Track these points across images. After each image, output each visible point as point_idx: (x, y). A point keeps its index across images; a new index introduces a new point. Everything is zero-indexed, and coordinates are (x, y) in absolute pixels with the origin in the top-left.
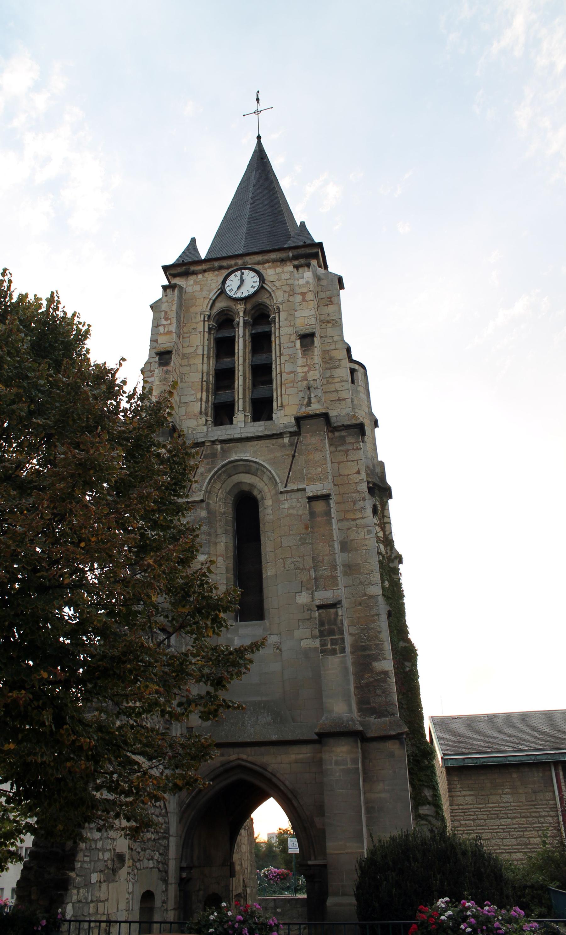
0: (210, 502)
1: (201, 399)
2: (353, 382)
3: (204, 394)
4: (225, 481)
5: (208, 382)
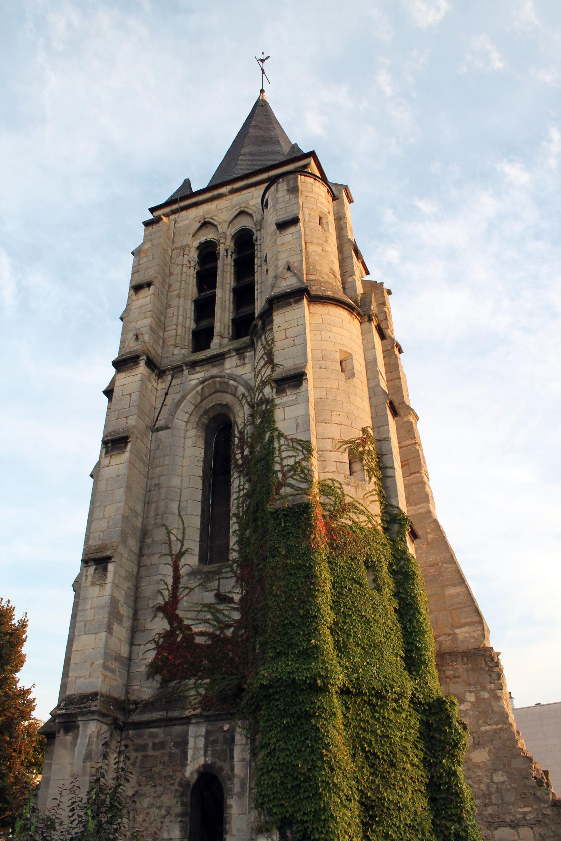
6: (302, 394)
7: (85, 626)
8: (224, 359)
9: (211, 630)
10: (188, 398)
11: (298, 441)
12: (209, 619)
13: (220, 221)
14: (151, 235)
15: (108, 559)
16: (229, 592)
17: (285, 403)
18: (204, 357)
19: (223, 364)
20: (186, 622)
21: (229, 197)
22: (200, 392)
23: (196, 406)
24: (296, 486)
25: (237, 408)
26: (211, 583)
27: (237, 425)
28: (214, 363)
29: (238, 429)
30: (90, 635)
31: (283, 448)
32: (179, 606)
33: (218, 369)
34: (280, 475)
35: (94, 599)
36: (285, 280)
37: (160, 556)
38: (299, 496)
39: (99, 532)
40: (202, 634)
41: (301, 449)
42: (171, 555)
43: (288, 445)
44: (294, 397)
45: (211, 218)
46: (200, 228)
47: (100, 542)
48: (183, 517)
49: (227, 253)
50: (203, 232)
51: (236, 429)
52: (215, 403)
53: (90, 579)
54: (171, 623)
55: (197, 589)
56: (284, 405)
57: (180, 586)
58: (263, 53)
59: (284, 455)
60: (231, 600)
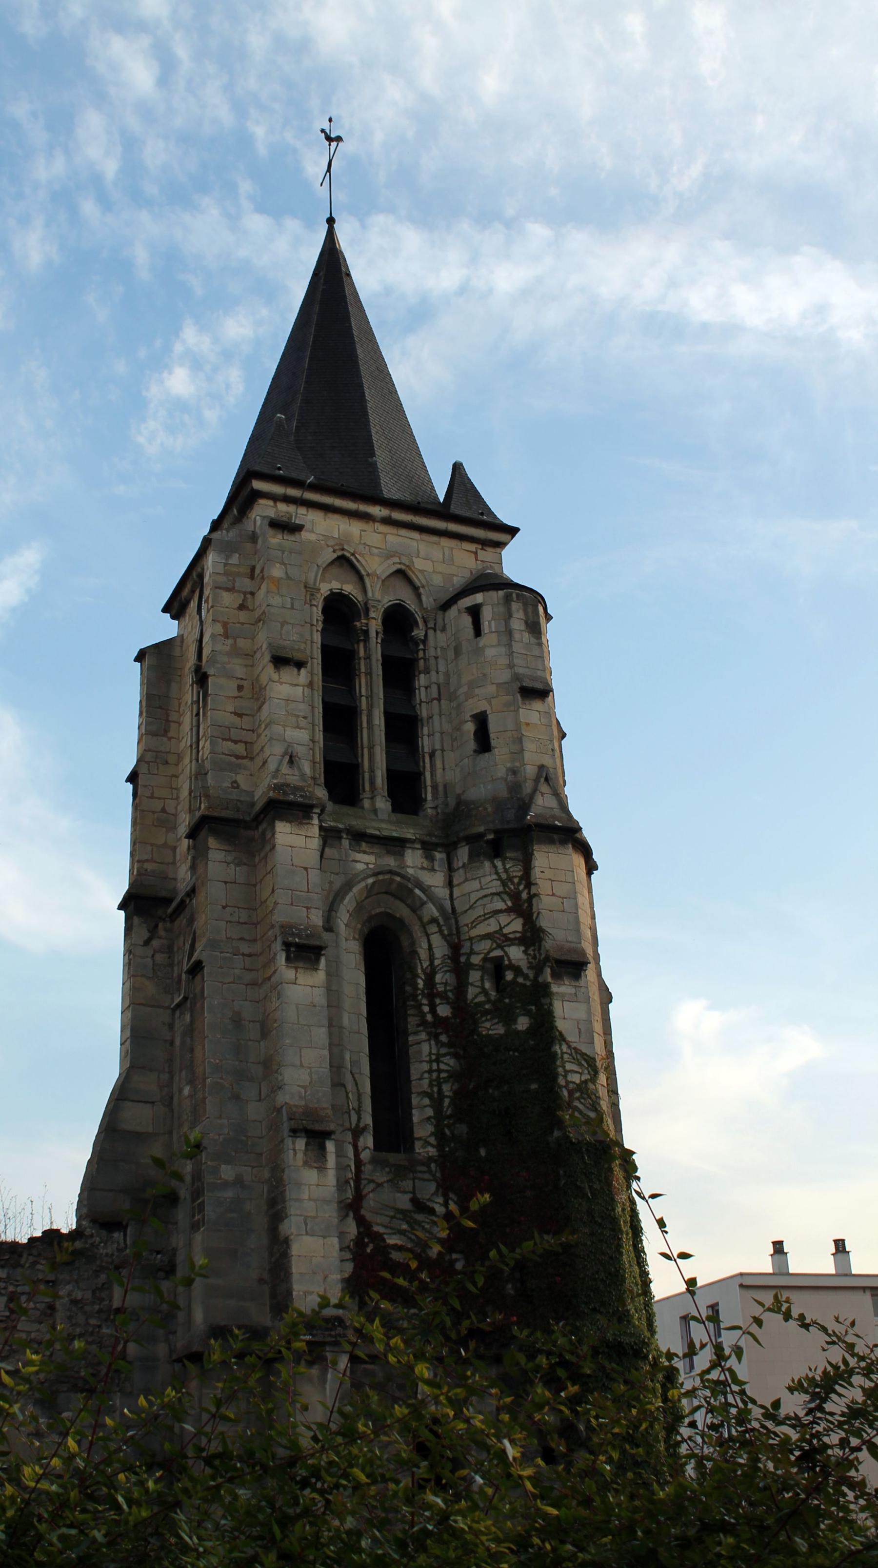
2: (478, 632)
6: (583, 990)
7: (306, 1224)
9: (409, 1246)
10: (355, 889)
11: (583, 1055)
12: (405, 1231)
13: (370, 572)
14: (283, 552)
15: (327, 1135)
16: (429, 1200)
18: (377, 833)
19: (402, 855)
20: (376, 1228)
21: (377, 525)
22: (369, 887)
23: (358, 904)
24: (585, 1112)
25: (417, 932)
26: (404, 1182)
27: (420, 961)
30: (315, 1238)
31: (566, 1056)
32: (365, 1204)
33: (395, 860)
34: (565, 1093)
35: (312, 1187)
36: (542, 796)
37: (343, 1131)
39: (299, 1086)
40: (399, 1248)
41: (586, 1066)
42: (350, 1129)
43: (571, 1055)
44: (573, 991)
45: (353, 554)
46: (332, 563)
47: (303, 1103)
48: (356, 1076)
49: (377, 639)
50: (335, 570)
51: (419, 964)
52: (382, 910)
53: (300, 1156)
54: (358, 1226)
55: (385, 1185)
56: (563, 998)
57: (363, 1177)
59: (568, 1066)
60: (432, 1211)
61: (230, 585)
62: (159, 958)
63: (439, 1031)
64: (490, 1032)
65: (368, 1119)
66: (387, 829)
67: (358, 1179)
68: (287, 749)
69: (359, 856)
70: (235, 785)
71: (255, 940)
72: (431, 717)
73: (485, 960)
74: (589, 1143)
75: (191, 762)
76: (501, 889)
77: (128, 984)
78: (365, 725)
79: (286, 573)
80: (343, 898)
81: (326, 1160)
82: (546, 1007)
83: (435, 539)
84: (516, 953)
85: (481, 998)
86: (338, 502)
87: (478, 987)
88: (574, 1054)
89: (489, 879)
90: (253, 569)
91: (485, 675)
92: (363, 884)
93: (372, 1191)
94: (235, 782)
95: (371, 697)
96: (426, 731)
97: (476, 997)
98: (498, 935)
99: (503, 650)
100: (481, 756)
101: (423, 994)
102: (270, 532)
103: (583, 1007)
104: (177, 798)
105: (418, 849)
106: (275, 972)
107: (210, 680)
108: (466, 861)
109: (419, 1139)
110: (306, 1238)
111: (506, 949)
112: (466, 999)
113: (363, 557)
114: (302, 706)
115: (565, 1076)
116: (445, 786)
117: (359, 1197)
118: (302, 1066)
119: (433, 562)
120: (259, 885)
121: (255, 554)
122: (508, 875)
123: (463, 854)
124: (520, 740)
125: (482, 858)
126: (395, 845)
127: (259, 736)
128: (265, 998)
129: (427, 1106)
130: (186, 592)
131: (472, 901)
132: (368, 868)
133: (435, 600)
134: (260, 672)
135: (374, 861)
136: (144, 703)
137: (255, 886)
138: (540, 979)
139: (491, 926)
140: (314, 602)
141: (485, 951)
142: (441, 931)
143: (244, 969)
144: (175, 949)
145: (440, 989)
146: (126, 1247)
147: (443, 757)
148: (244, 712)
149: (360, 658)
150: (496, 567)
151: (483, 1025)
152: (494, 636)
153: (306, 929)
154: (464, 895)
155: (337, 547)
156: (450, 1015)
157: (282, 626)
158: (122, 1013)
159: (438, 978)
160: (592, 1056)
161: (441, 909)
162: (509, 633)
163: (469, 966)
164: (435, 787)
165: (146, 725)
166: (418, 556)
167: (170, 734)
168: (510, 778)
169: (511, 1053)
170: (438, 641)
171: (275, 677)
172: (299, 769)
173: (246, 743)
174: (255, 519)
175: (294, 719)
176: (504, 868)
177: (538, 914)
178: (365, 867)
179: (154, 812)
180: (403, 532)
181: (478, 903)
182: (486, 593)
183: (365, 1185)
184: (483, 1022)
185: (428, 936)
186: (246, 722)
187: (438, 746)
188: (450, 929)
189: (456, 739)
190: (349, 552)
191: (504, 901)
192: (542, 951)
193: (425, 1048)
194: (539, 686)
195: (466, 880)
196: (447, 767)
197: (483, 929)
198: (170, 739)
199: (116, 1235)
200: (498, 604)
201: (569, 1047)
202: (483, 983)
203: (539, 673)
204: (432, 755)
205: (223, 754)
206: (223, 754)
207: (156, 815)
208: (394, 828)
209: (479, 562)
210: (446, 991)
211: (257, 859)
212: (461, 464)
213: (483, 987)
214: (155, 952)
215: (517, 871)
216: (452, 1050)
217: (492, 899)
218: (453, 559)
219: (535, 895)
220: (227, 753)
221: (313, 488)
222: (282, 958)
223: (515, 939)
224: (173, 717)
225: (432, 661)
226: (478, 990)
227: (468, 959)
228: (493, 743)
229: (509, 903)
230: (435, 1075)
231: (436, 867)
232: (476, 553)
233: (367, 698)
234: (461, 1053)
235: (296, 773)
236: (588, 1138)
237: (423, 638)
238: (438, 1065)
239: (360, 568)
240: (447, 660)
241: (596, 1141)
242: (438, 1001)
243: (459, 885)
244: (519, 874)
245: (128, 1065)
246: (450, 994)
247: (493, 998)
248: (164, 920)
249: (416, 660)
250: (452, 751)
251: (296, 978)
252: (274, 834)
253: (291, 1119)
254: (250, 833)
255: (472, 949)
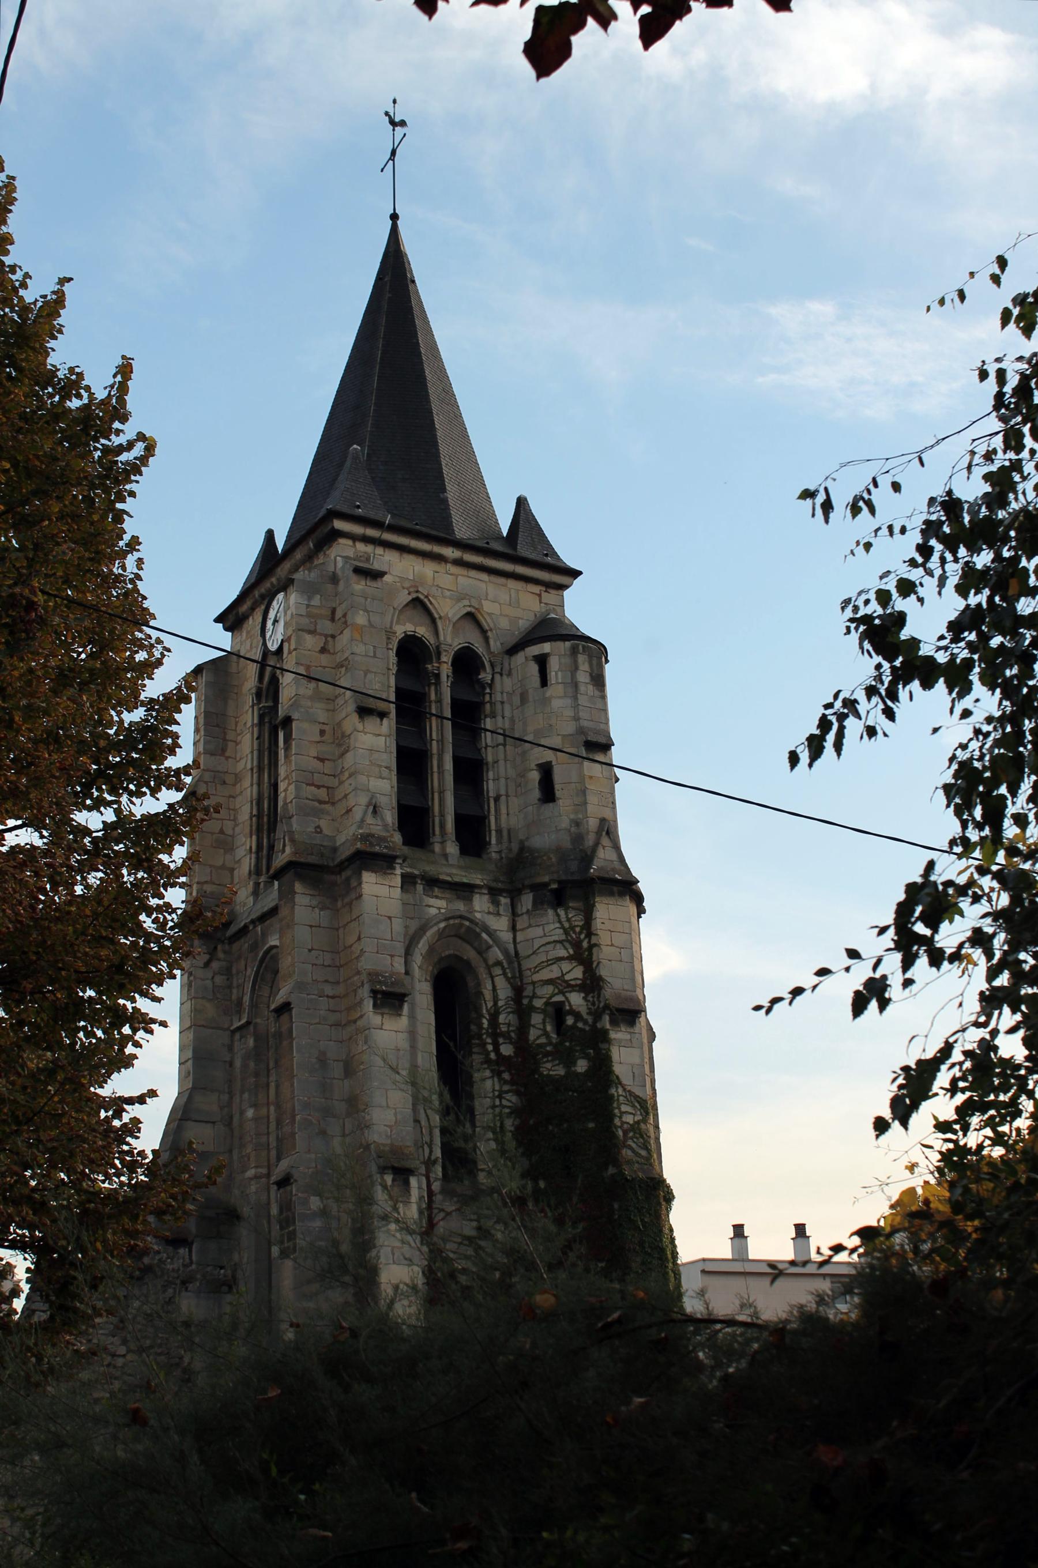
0: (258, 1020)
1: (251, 847)
3: (254, 837)
4: (273, 982)
5: (259, 816)
6: (637, 1036)
7: (393, 1254)
8: (473, 892)
10: (429, 933)
11: (636, 1097)
14: (366, 598)
17: (620, 1041)
18: (449, 879)
21: (449, 566)
23: (430, 947)
27: (485, 1001)
28: (459, 892)
29: (487, 1007)
31: (621, 1098)
34: (620, 1133)
38: (646, 1167)
43: (626, 1097)
44: (628, 1037)
45: (426, 597)
46: (407, 605)
47: (389, 1142)
52: (452, 952)
55: (454, 1213)
57: (434, 1206)
58: (395, 102)
59: (624, 1108)
61: (312, 629)
62: (219, 980)
63: (502, 1068)
64: (551, 1073)
65: (438, 1153)
66: (457, 875)
67: (430, 1207)
68: (371, 799)
69: (432, 901)
70: (319, 830)
71: (338, 983)
72: (496, 762)
73: (547, 1004)
74: (641, 1179)
75: (252, 785)
76: (563, 937)
77: (188, 1005)
78: (435, 769)
79: (369, 621)
80: (418, 943)
81: (410, 1195)
82: (604, 1052)
83: (502, 580)
84: (576, 1000)
85: (543, 1040)
86: (415, 544)
87: (540, 1029)
88: (628, 1097)
89: (552, 926)
90: (334, 611)
91: (551, 726)
92: (435, 929)
93: (442, 1220)
94: (318, 827)
95: (442, 741)
96: (491, 775)
97: (538, 1038)
98: (559, 982)
99: (569, 701)
100: (546, 805)
101: (487, 1033)
102: (354, 578)
103: (636, 1052)
104: (235, 820)
105: (484, 894)
106: (361, 1016)
107: (294, 724)
108: (530, 907)
109: (482, 1170)
110: (394, 1267)
111: (567, 995)
112: (527, 1040)
113: (436, 599)
114: (385, 756)
115: (620, 1117)
116: (509, 831)
117: (431, 1225)
118: (388, 1107)
119: (500, 604)
120: (342, 929)
121: (336, 596)
122: (570, 924)
123: (527, 901)
124: (584, 792)
125: (546, 906)
126: (464, 890)
127: (341, 783)
128: (350, 1038)
129: (489, 1140)
130: (244, 608)
131: (536, 947)
132: (440, 913)
133: (502, 644)
134: (344, 719)
135: (445, 906)
136: (201, 721)
137: (337, 929)
138: (599, 1025)
139: (553, 972)
140: (390, 646)
141: (548, 996)
142: (505, 974)
143: (329, 1010)
144: (234, 971)
145: (503, 1029)
146: (191, 1263)
147: (507, 802)
148: (328, 757)
149: (431, 702)
150: (558, 609)
151: (544, 1065)
152: (561, 686)
153: (391, 976)
154: (528, 940)
155: (412, 590)
156: (512, 1054)
157: (365, 675)
158: (180, 1033)
159: (502, 1018)
160: (644, 1098)
161: (505, 952)
162: (575, 685)
163: (532, 1009)
164: (499, 831)
165: (205, 743)
166: (487, 599)
167: (227, 754)
168: (573, 829)
169: (570, 1093)
170: (504, 685)
171: (360, 726)
172: (383, 819)
173: (328, 788)
174: (335, 559)
175: (377, 769)
176: (567, 916)
177: (599, 963)
178: (438, 912)
179: (212, 834)
180: (473, 573)
181: (541, 949)
182: (553, 643)
183: (436, 1214)
184: (544, 1063)
185: (492, 978)
186: (328, 768)
187: (503, 792)
188: (513, 973)
189: (520, 785)
190: (423, 594)
191: (566, 949)
192: (601, 999)
193: (489, 1083)
194: (602, 740)
195: (530, 926)
196: (511, 812)
197: (545, 974)
198: (227, 758)
199: (181, 1251)
200: (565, 655)
201: (624, 1090)
202: (544, 1026)
203: (602, 726)
204: (497, 799)
205: (307, 799)
206: (307, 799)
207: (214, 836)
208: (464, 874)
209: (542, 605)
210: (509, 1032)
211: (339, 904)
212: (526, 499)
213: (544, 1030)
214: (215, 974)
215: (578, 921)
216: (514, 1087)
217: (555, 946)
218: (518, 603)
219: (595, 945)
220: (310, 797)
221: (392, 528)
222: (369, 1005)
223: (576, 985)
224: (230, 736)
225: (499, 706)
226: (540, 1032)
227: (531, 1001)
228: (558, 794)
229: (571, 952)
230: (497, 1110)
231: (501, 912)
232: (540, 595)
233: (437, 741)
234: (523, 1090)
235: (380, 823)
236: (640, 1175)
237: (489, 682)
238: (501, 1101)
239: (433, 611)
240: (512, 706)
241: (648, 1178)
242: (501, 1040)
243: (522, 930)
244: (581, 923)
245: (191, 1086)
246: (513, 1035)
247: (554, 1041)
248: (223, 942)
249: (483, 703)
250: (516, 796)
251: (382, 1024)
252: (360, 884)
253: (380, 1157)
254: (333, 877)
255: (534, 993)
